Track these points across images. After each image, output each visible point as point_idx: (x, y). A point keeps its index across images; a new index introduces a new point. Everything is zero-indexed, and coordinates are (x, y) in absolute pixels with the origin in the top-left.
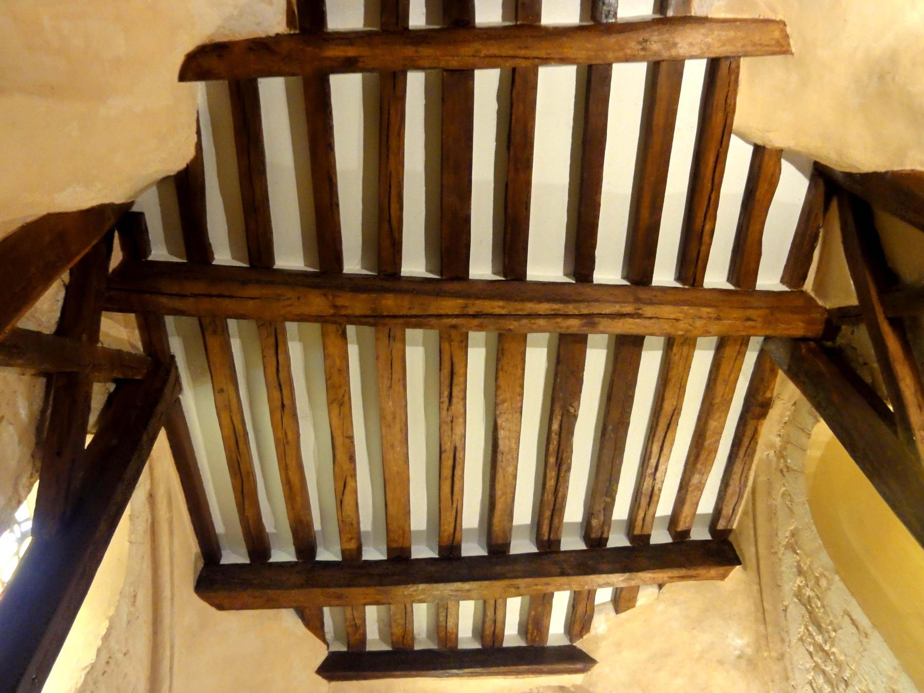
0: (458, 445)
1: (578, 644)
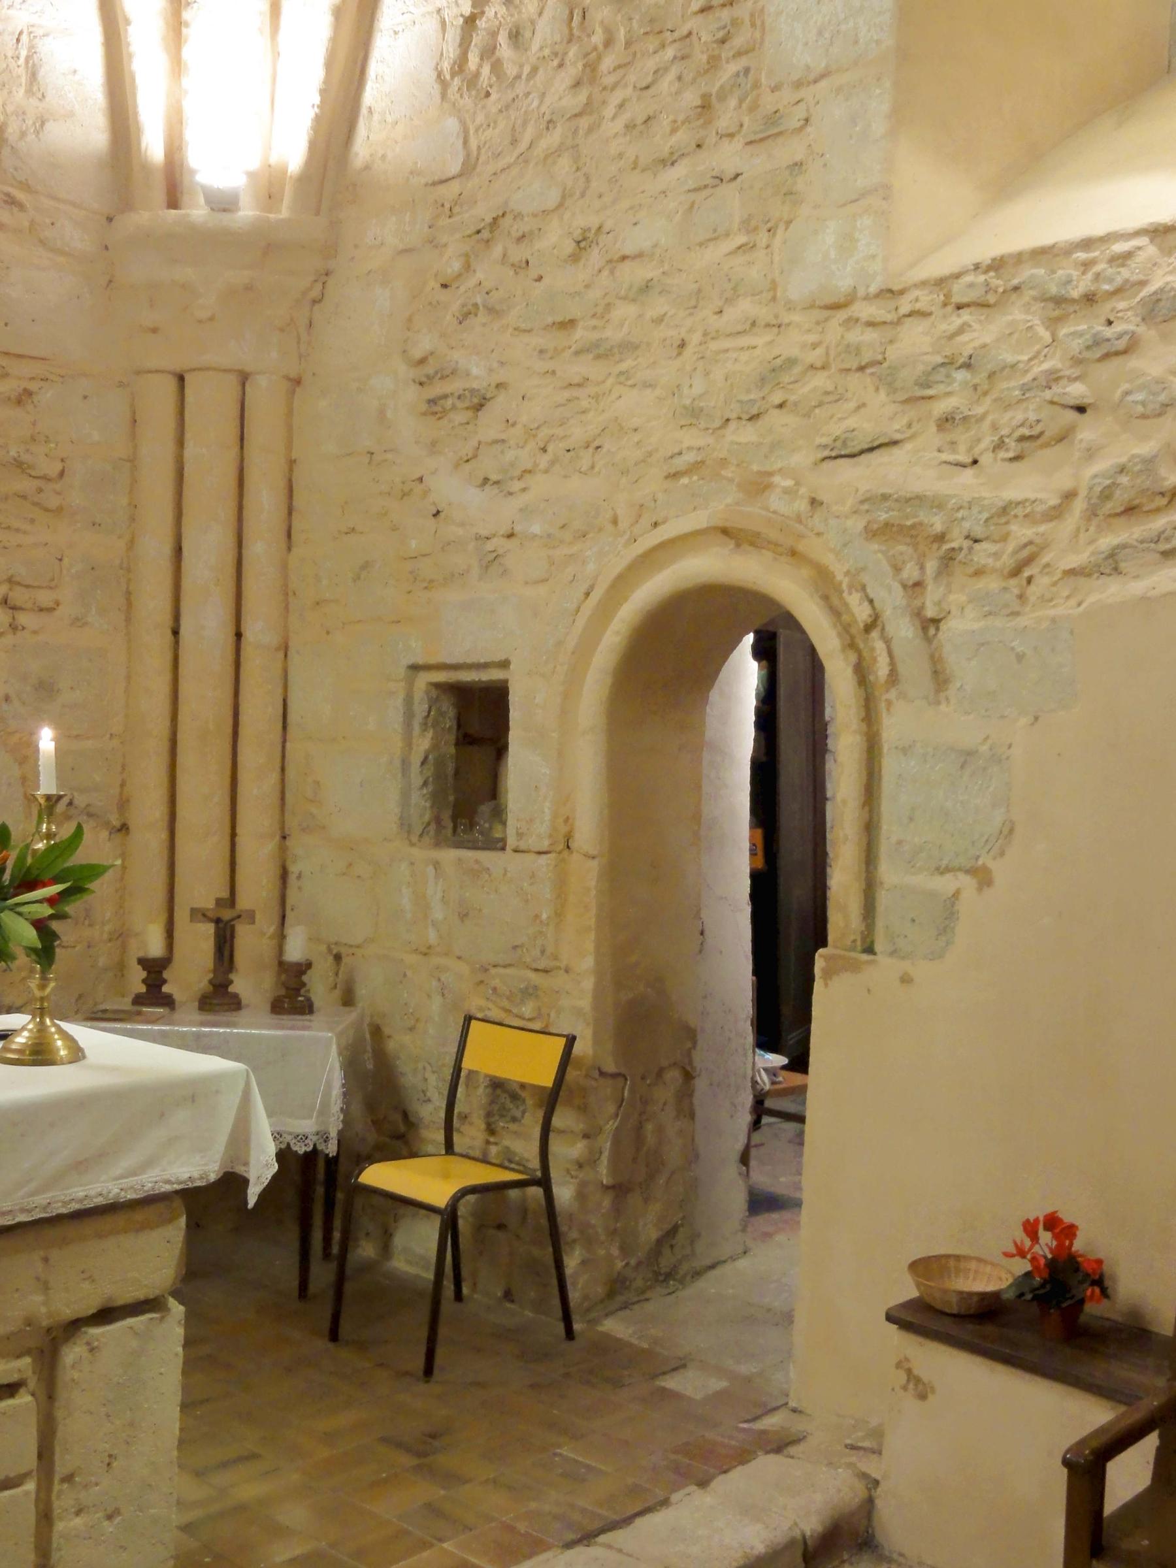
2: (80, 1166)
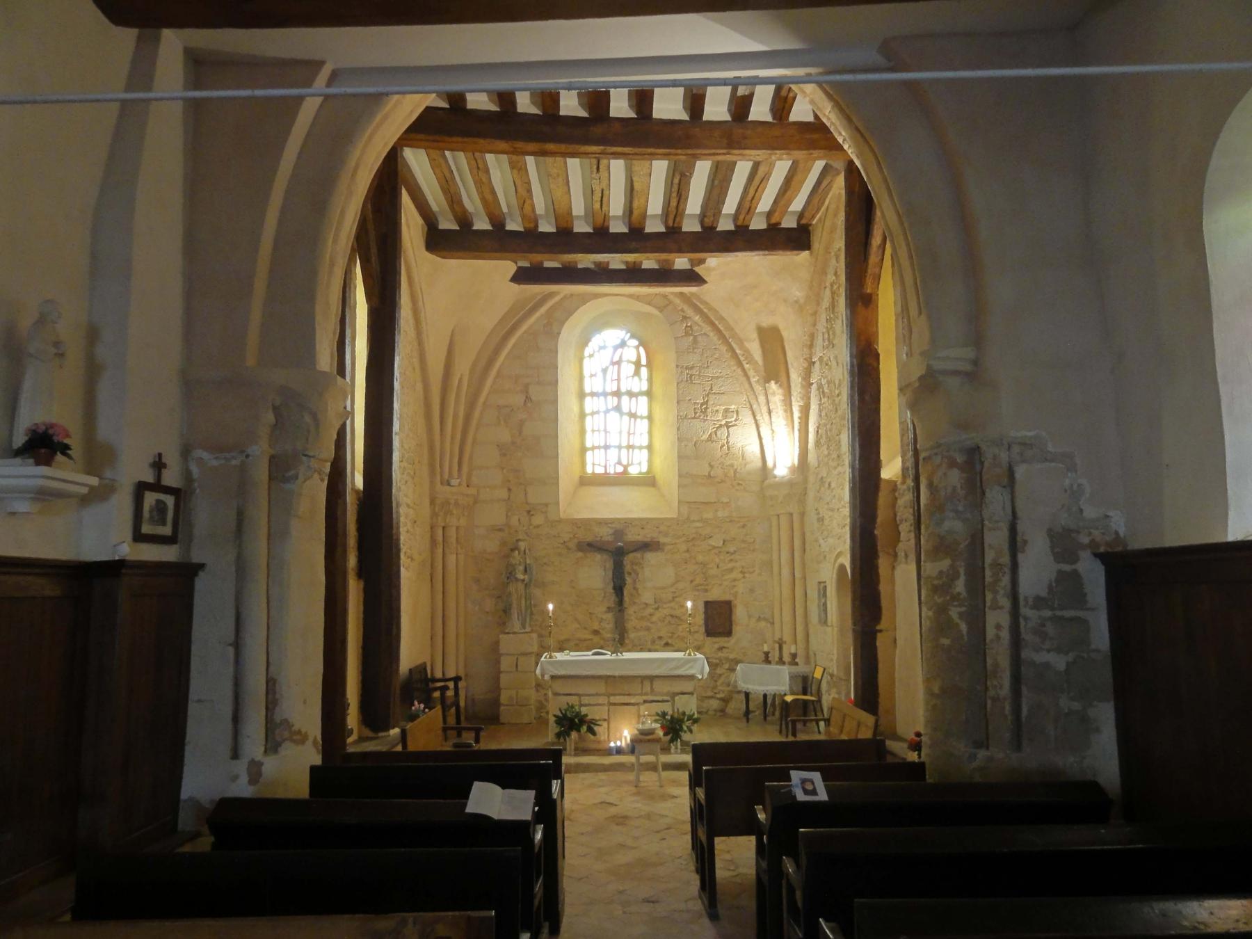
1: (696, 269)
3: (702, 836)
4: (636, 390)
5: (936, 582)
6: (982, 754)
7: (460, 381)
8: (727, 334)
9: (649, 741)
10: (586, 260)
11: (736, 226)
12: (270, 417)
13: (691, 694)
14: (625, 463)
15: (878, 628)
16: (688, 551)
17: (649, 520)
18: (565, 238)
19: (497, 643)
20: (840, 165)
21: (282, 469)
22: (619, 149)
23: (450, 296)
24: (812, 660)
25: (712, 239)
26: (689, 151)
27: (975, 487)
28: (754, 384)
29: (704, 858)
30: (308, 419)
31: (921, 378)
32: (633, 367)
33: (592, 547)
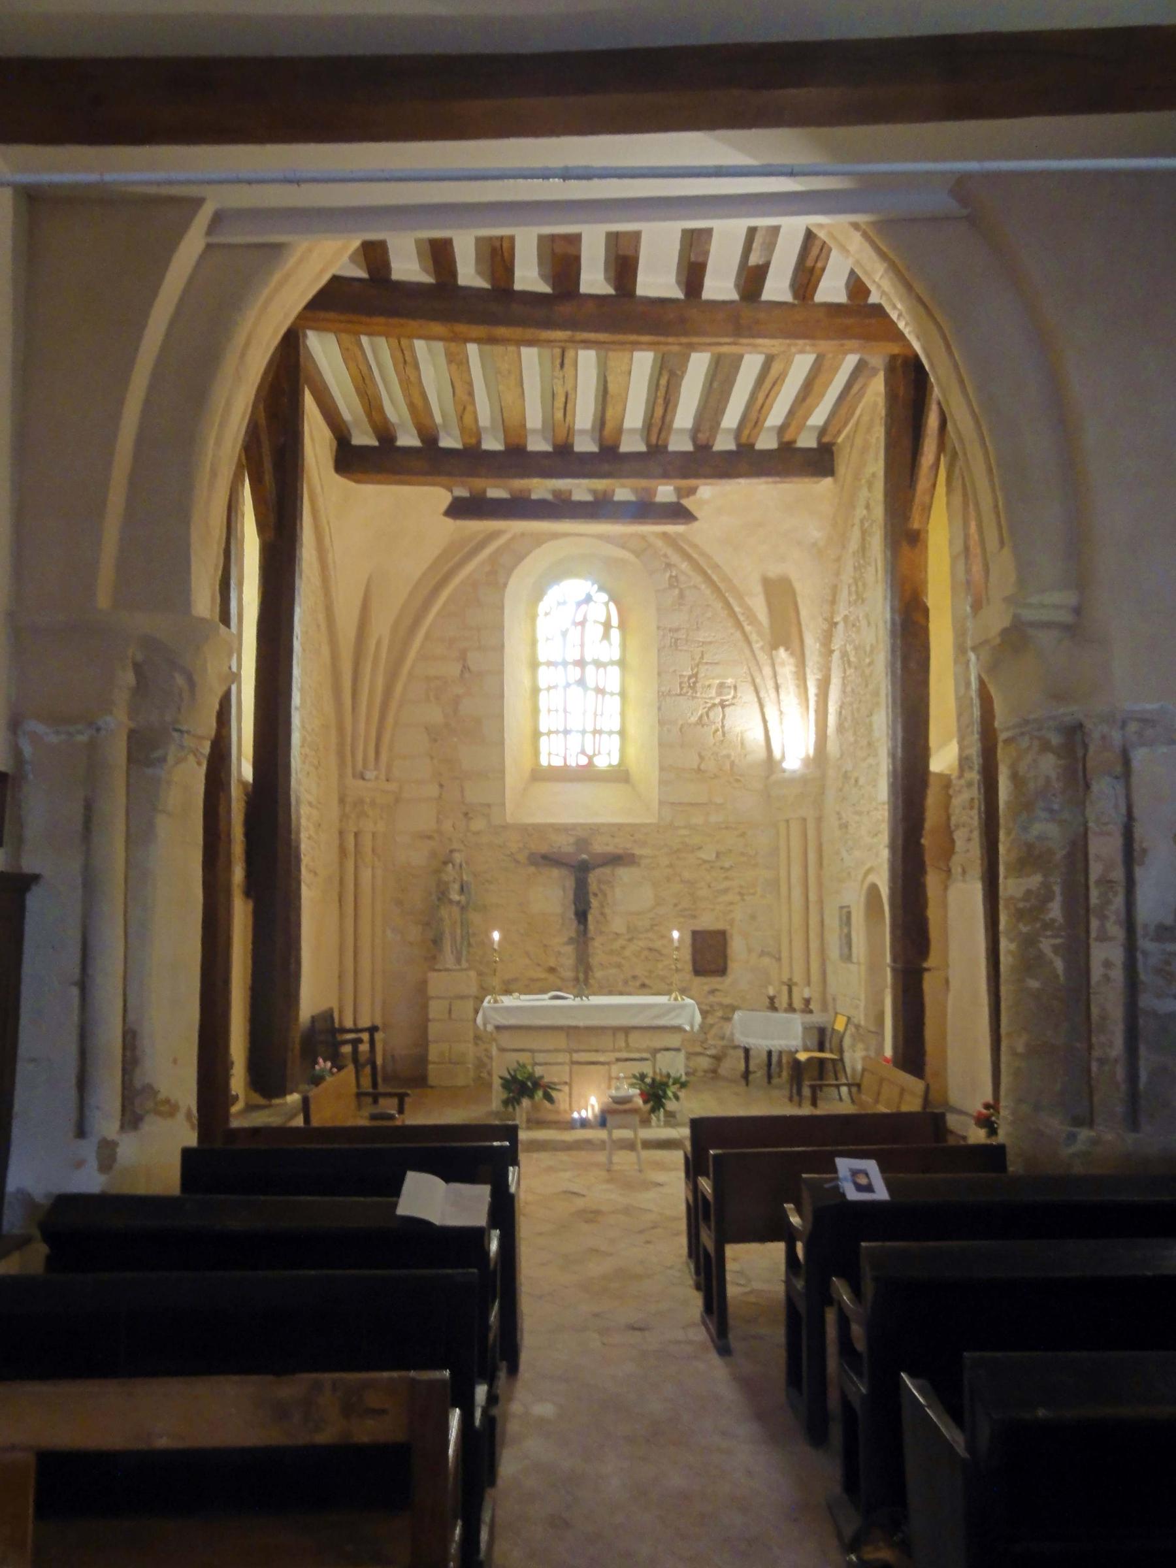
0: (570, 392)
1: (685, 502)
2: (658, 1017)
3: (707, 1240)
4: (605, 659)
5: (1021, 905)
6: (1084, 1134)
7: (379, 643)
8: (722, 586)
9: (625, 1112)
10: (541, 488)
11: (739, 445)
12: (129, 678)
13: (678, 1050)
14: (590, 752)
15: (925, 965)
16: (671, 866)
17: (620, 826)
18: (515, 458)
19: (425, 982)
20: (878, 361)
21: (146, 749)
22: (592, 336)
23: (363, 531)
24: (830, 1007)
25: (705, 462)
26: (684, 340)
27: (1077, 778)
28: (757, 652)
29: (709, 1273)
30: (180, 680)
31: (1005, 632)
32: (601, 629)
33: (549, 860)
